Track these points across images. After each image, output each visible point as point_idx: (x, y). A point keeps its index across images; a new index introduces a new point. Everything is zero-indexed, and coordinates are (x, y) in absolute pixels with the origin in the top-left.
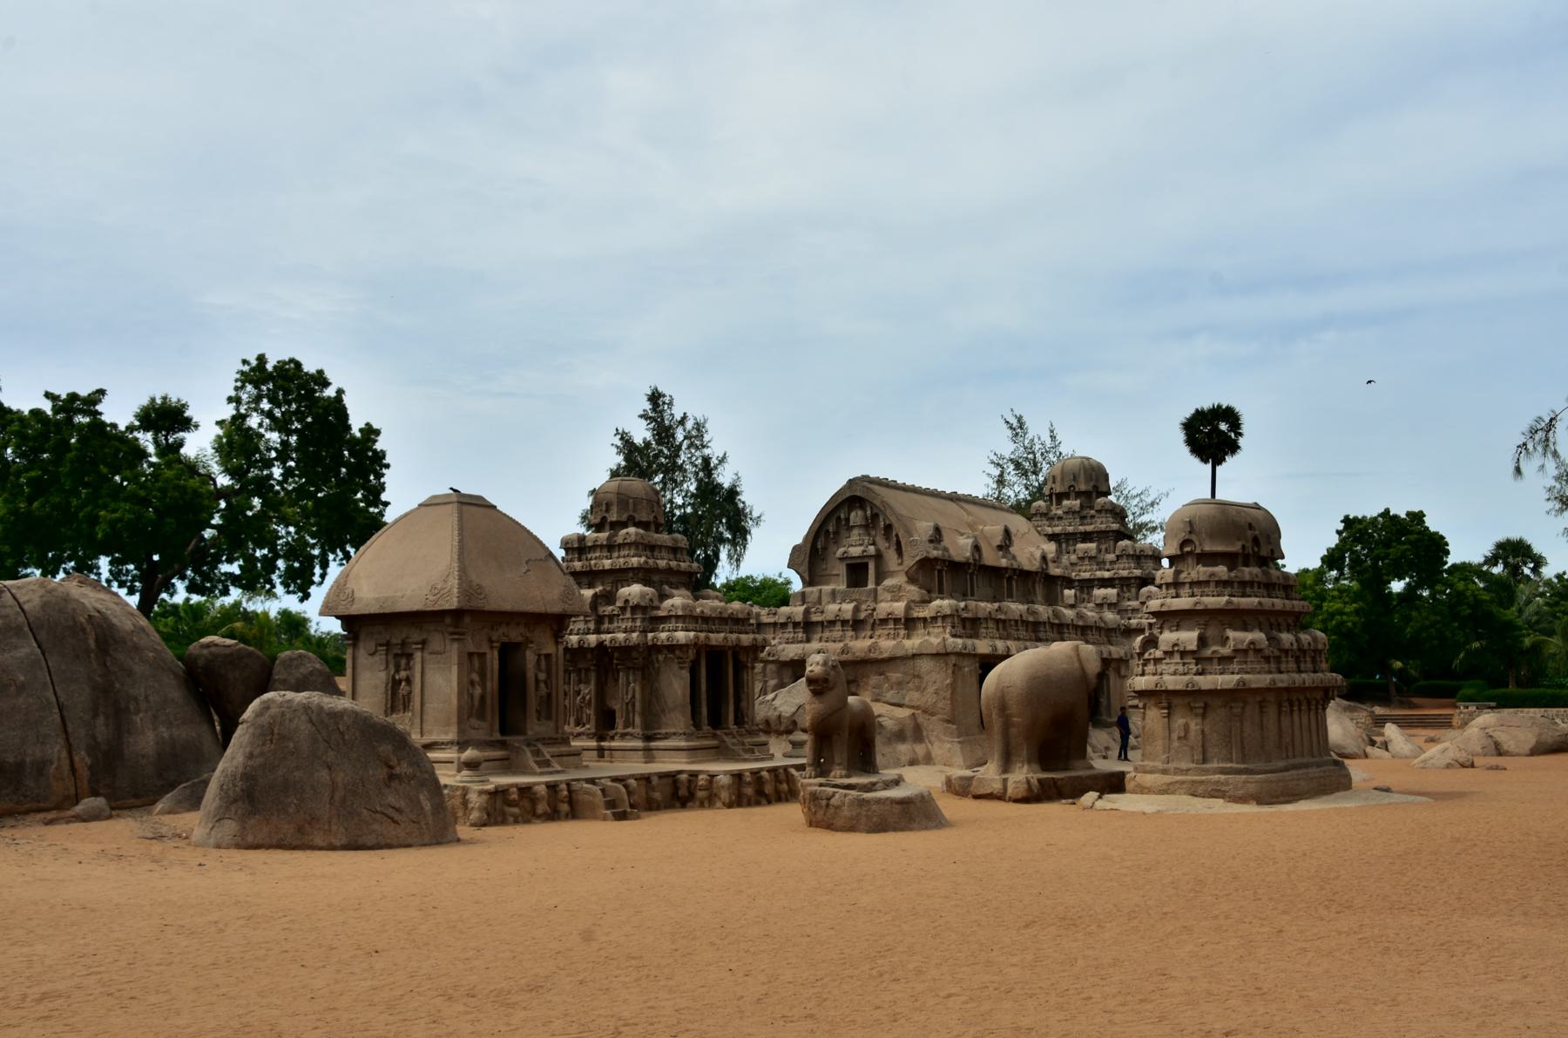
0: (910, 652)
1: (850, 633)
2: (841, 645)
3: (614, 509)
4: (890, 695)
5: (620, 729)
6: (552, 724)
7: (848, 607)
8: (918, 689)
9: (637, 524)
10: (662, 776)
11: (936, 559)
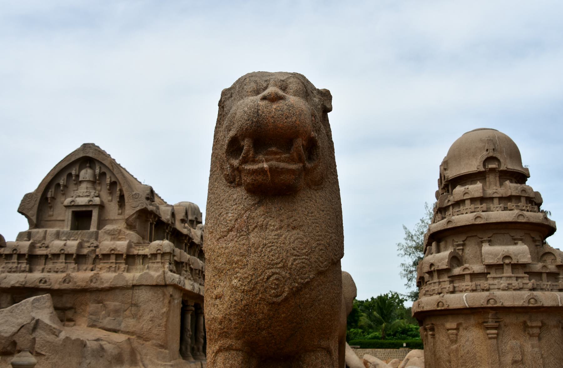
0: (130, 283)
1: (73, 265)
2: (64, 275)
4: (107, 322)
7: (75, 243)
8: (134, 316)
11: (151, 213)
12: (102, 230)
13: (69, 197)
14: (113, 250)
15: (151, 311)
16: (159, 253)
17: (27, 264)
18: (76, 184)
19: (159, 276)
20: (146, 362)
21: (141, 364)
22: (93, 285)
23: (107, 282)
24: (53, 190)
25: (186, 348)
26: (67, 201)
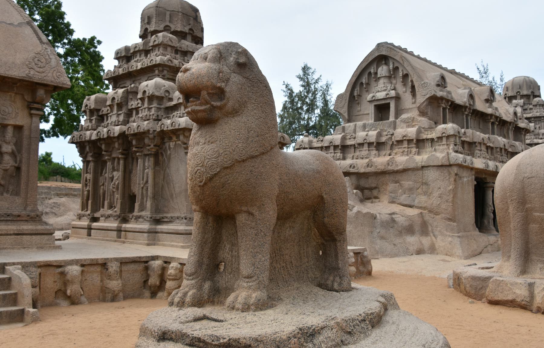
0: (420, 165)
1: (374, 152)
2: (367, 160)
3: (154, 20)
4: (403, 198)
5: (136, 213)
6: (18, 200)
8: (425, 193)
9: (175, 33)
10: (124, 262)
11: (442, 98)
12: (399, 119)
13: (371, 93)
14: (405, 136)
15: (439, 188)
16: (444, 136)
17: (341, 153)
18: (376, 81)
19: (443, 157)
20: (437, 233)
21: (431, 234)
22: (390, 168)
23: (401, 165)
24: (358, 89)
25: (489, 222)
26: (369, 97)
